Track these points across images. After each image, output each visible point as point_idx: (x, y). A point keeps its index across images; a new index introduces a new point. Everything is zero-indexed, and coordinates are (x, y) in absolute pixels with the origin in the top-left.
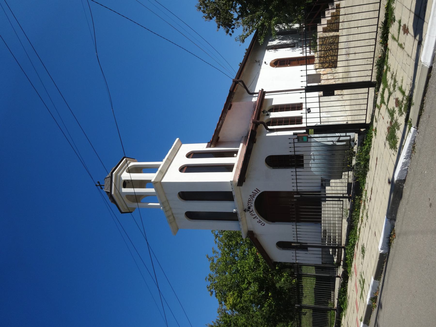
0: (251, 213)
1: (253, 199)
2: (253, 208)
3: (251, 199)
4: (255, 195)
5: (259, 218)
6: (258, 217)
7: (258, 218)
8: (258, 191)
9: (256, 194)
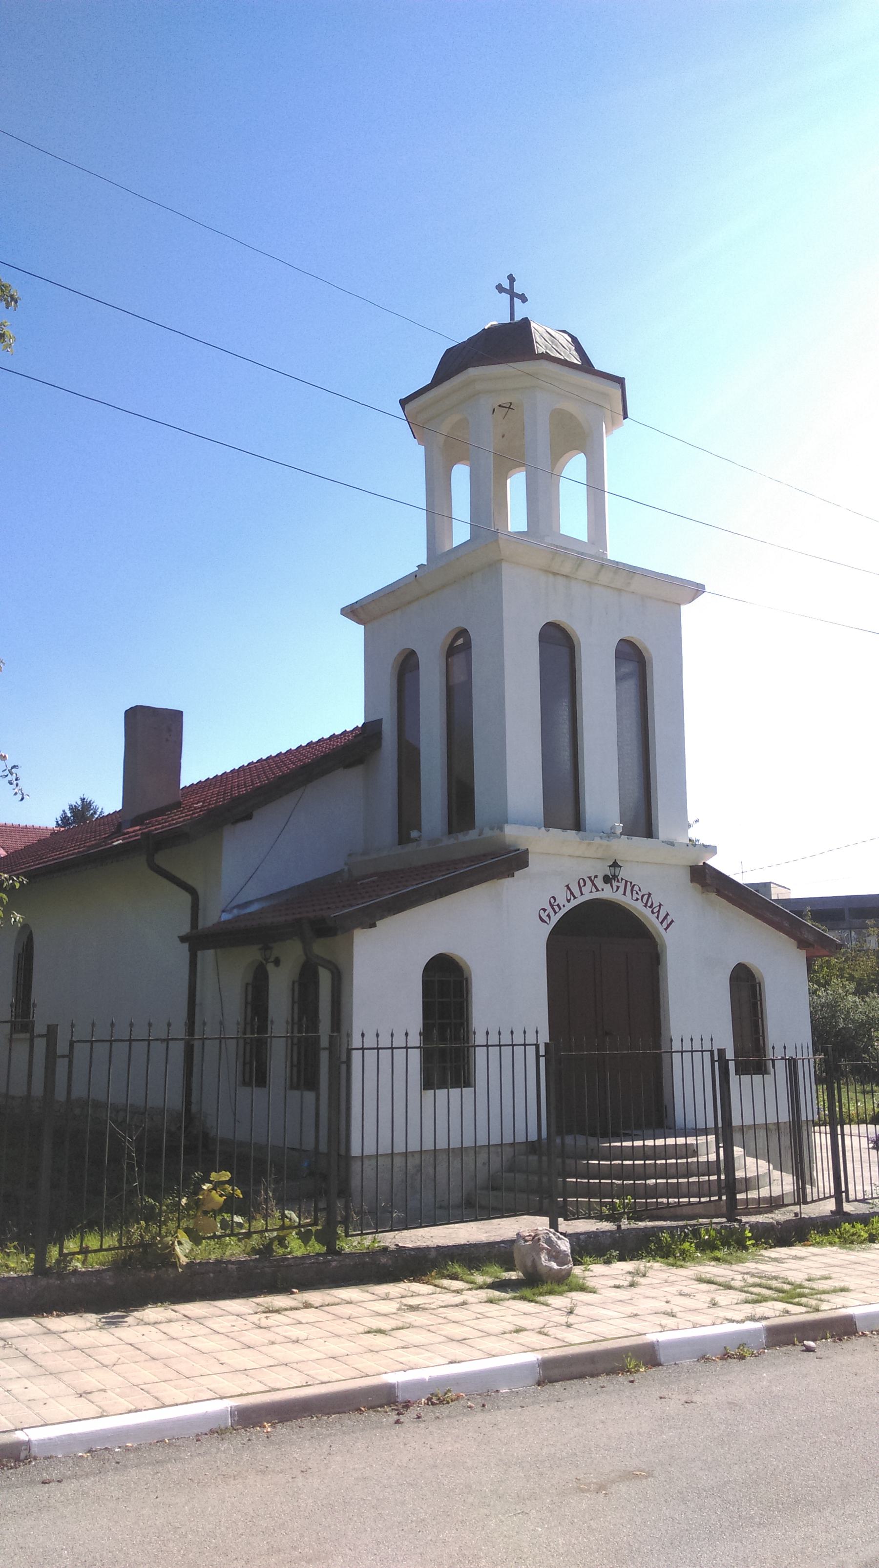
0: (589, 883)
1: (640, 901)
2: (607, 893)
3: (637, 893)
4: (653, 912)
5: (569, 906)
6: (574, 903)
7: (569, 901)
8: (665, 925)
9: (656, 914)
